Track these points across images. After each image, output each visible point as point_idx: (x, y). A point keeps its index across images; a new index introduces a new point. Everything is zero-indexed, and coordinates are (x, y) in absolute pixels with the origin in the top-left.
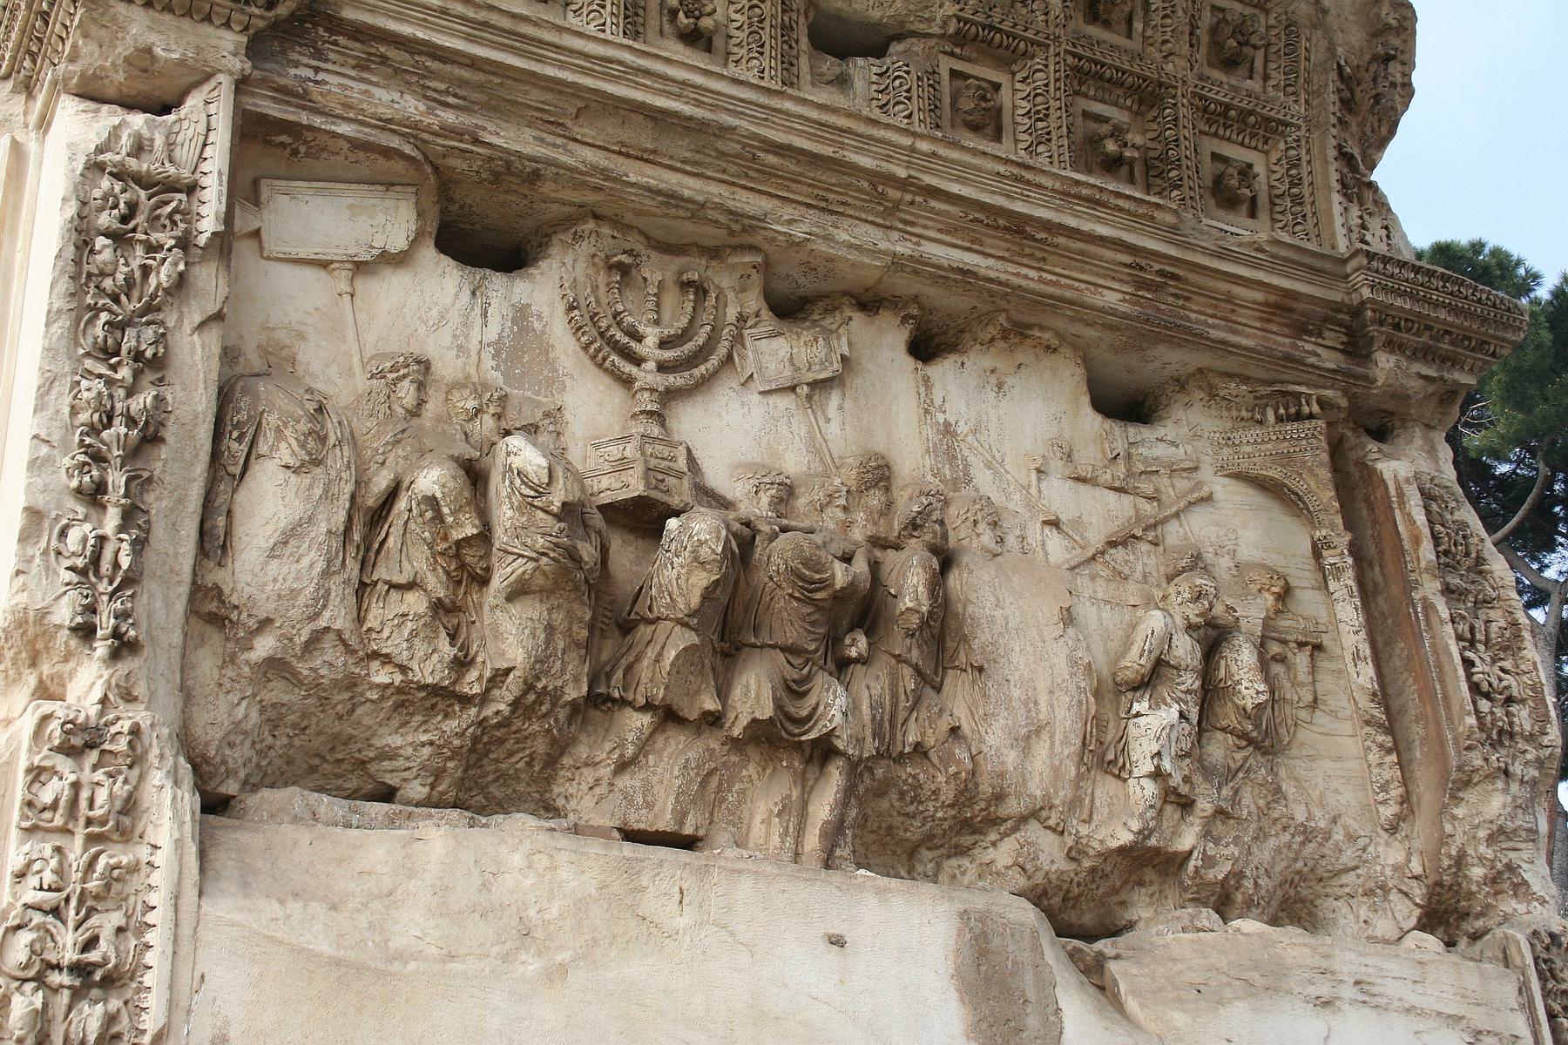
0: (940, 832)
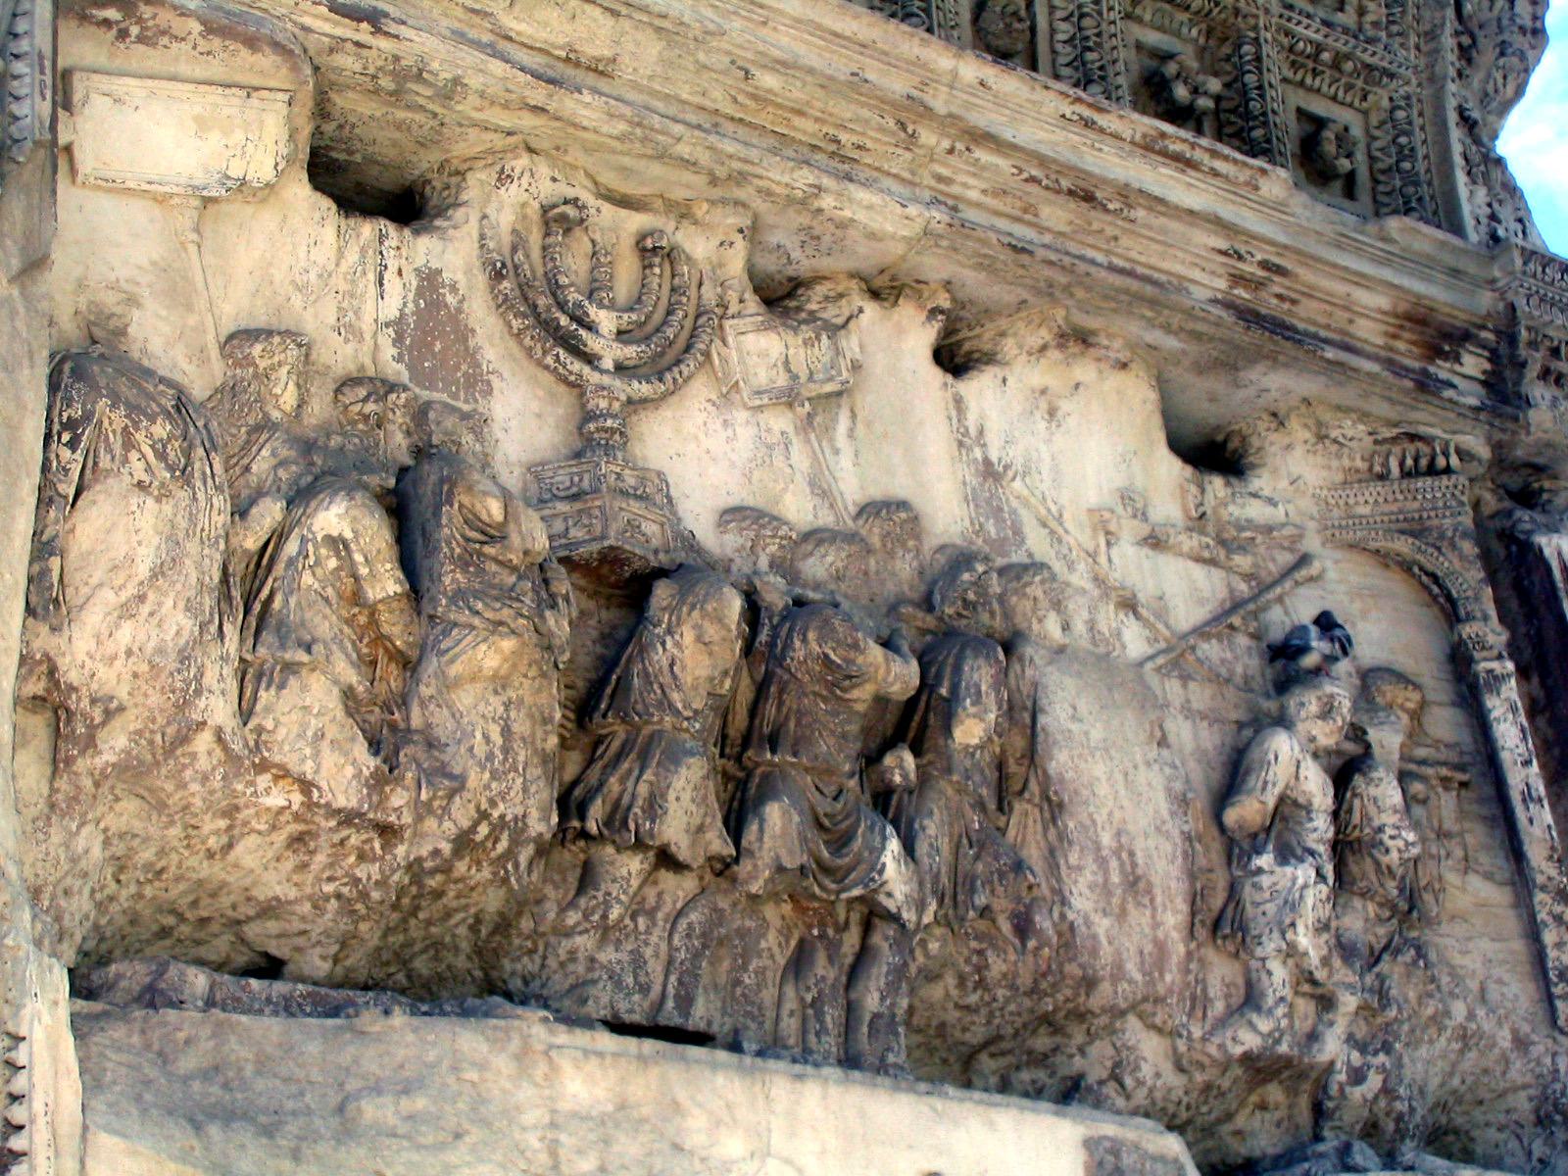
0: (1010, 1030)
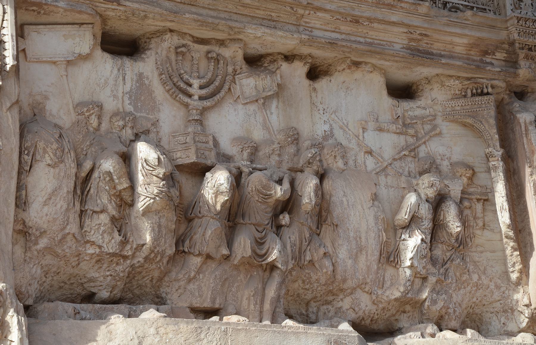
0: (319, 295)
